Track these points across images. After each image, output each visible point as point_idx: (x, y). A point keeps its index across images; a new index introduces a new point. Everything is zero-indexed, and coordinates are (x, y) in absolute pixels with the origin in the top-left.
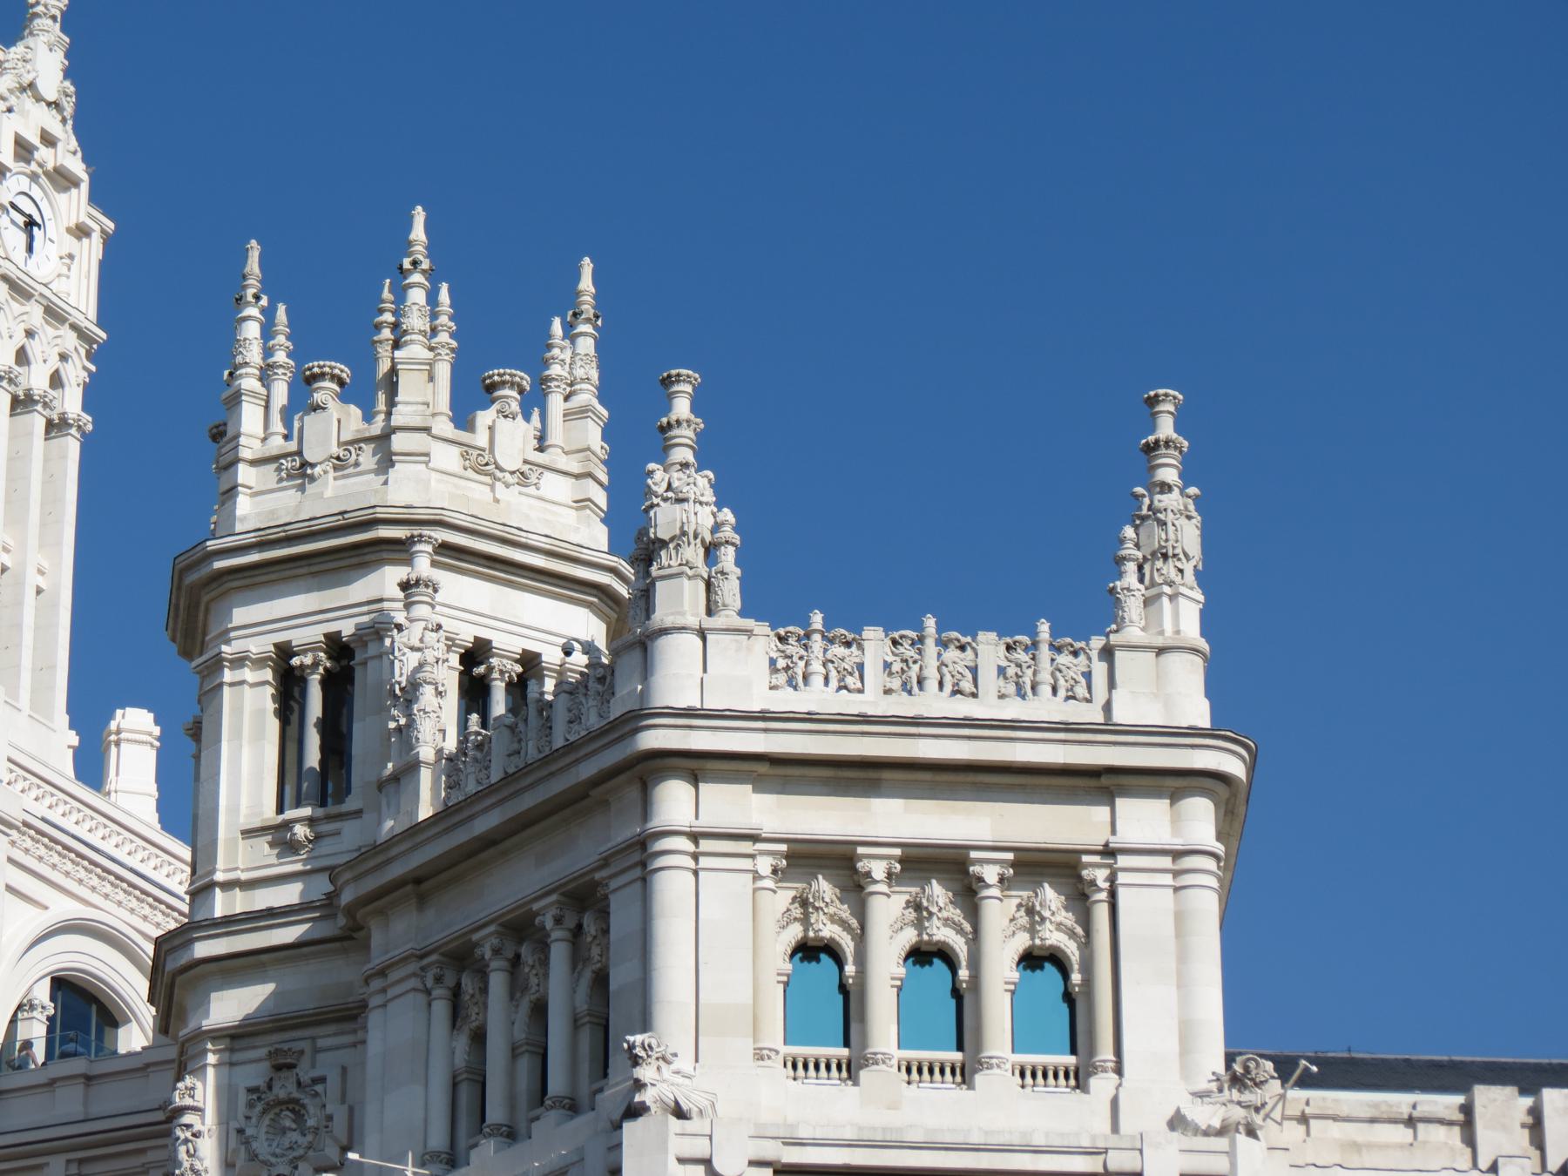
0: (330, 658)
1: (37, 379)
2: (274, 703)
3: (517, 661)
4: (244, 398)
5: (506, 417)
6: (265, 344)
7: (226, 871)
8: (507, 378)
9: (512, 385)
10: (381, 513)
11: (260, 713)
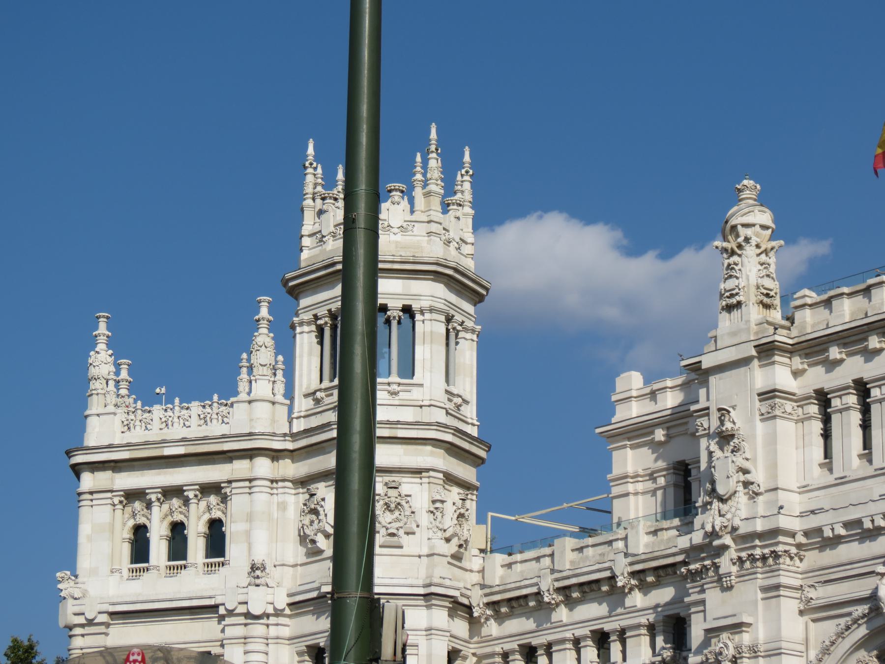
0: (331, 320)
3: (400, 311)
7: (298, 412)
8: (393, 188)
9: (396, 190)
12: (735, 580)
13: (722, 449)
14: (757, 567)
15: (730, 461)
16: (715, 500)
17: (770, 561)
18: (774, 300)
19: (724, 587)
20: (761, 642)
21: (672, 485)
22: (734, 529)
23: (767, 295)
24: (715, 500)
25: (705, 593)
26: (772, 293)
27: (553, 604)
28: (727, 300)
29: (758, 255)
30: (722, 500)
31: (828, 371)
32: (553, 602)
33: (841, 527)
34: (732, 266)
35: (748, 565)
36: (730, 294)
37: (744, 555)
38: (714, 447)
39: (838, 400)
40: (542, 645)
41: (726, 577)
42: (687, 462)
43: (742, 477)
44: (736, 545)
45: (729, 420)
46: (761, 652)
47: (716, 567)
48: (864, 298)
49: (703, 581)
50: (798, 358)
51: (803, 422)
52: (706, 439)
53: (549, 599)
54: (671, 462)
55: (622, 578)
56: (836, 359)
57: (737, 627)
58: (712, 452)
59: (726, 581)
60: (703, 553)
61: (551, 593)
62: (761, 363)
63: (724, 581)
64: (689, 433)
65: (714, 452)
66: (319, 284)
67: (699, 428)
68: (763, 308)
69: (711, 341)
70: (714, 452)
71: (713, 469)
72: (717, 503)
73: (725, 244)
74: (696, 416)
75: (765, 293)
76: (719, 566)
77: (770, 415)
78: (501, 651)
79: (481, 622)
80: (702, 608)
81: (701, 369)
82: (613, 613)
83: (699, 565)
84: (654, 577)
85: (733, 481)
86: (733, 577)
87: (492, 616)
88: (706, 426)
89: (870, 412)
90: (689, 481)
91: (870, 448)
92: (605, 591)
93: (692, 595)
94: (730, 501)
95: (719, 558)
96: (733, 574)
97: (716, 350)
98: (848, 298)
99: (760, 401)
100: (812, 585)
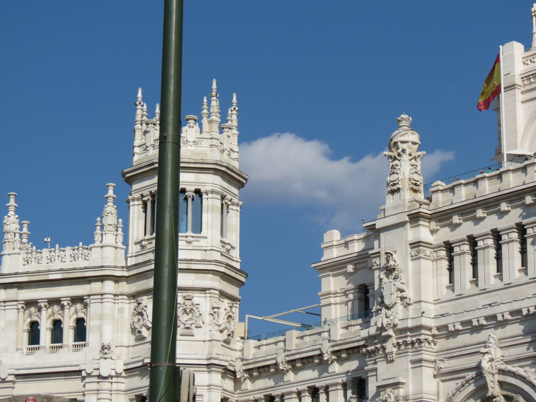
0: (152, 198)
2: (143, 209)
3: (193, 192)
7: (131, 253)
8: (189, 118)
9: (191, 119)
11: (139, 211)
12: (395, 356)
13: (387, 277)
14: (409, 349)
15: (393, 284)
16: (383, 308)
17: (417, 345)
18: (420, 187)
19: (389, 361)
20: (410, 394)
21: (358, 299)
22: (395, 326)
23: (416, 184)
24: (383, 308)
25: (377, 364)
26: (418, 183)
27: (285, 371)
28: (392, 187)
29: (410, 160)
30: (388, 308)
31: (452, 230)
32: (285, 369)
33: (459, 324)
34: (394, 166)
35: (403, 347)
36: (393, 184)
37: (401, 341)
38: (383, 276)
39: (458, 248)
40: (278, 396)
41: (390, 355)
42: (367, 285)
43: (400, 294)
44: (396, 335)
45: (392, 260)
46: (410, 400)
47: (384, 348)
49: (376, 357)
50: (434, 222)
51: (436, 261)
52: (378, 271)
53: (283, 367)
54: (358, 285)
55: (327, 355)
56: (457, 223)
57: (396, 385)
58: (382, 279)
59: (390, 357)
60: (376, 340)
61: (284, 364)
63: (388, 357)
64: (368, 267)
65: (383, 279)
67: (374, 264)
68: (413, 192)
69: (381, 212)
70: (383, 279)
71: (382, 289)
72: (384, 310)
73: (390, 153)
74: (372, 257)
76: (385, 348)
77: (417, 257)
78: (253, 399)
79: (241, 381)
80: (375, 373)
82: (322, 376)
83: (374, 347)
84: (346, 354)
85: (394, 297)
86: (394, 355)
87: (248, 378)
88: (378, 263)
89: (477, 255)
90: (368, 296)
91: (477, 277)
92: (317, 363)
93: (369, 365)
94: (392, 308)
95: (385, 343)
96: (394, 353)
97: (385, 217)
98: (464, 187)
99: (411, 248)
100: (442, 360)
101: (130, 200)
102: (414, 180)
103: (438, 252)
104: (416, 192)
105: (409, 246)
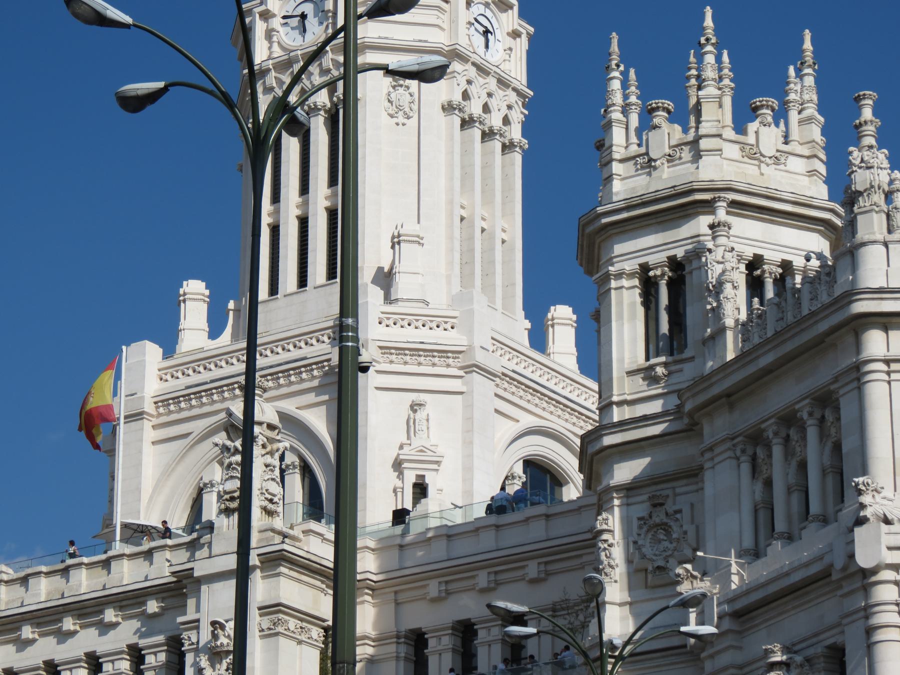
0: (671, 270)
1: (495, 121)
2: (641, 298)
3: (779, 266)
4: (613, 124)
5: (765, 125)
6: (624, 92)
7: (618, 395)
8: (764, 103)
9: (767, 107)
10: (696, 186)
11: (632, 305)
13: (213, 666)
21: (451, 650)
23: (271, 501)
26: (276, 499)
28: (227, 503)
29: (263, 456)
31: (19, 650)
34: (234, 466)
36: (230, 497)
38: (204, 662)
45: (224, 635)
48: (61, 578)
52: (193, 654)
62: (262, 575)
65: (205, 669)
66: (627, 228)
67: (186, 642)
69: (204, 547)
73: (228, 443)
74: (182, 628)
75: (269, 498)
81: (193, 577)
88: (194, 640)
90: (462, 648)
98: (46, 577)
101: (612, 277)
102: (270, 494)
103: (73, 670)
104: (270, 515)
105: (257, 612)
